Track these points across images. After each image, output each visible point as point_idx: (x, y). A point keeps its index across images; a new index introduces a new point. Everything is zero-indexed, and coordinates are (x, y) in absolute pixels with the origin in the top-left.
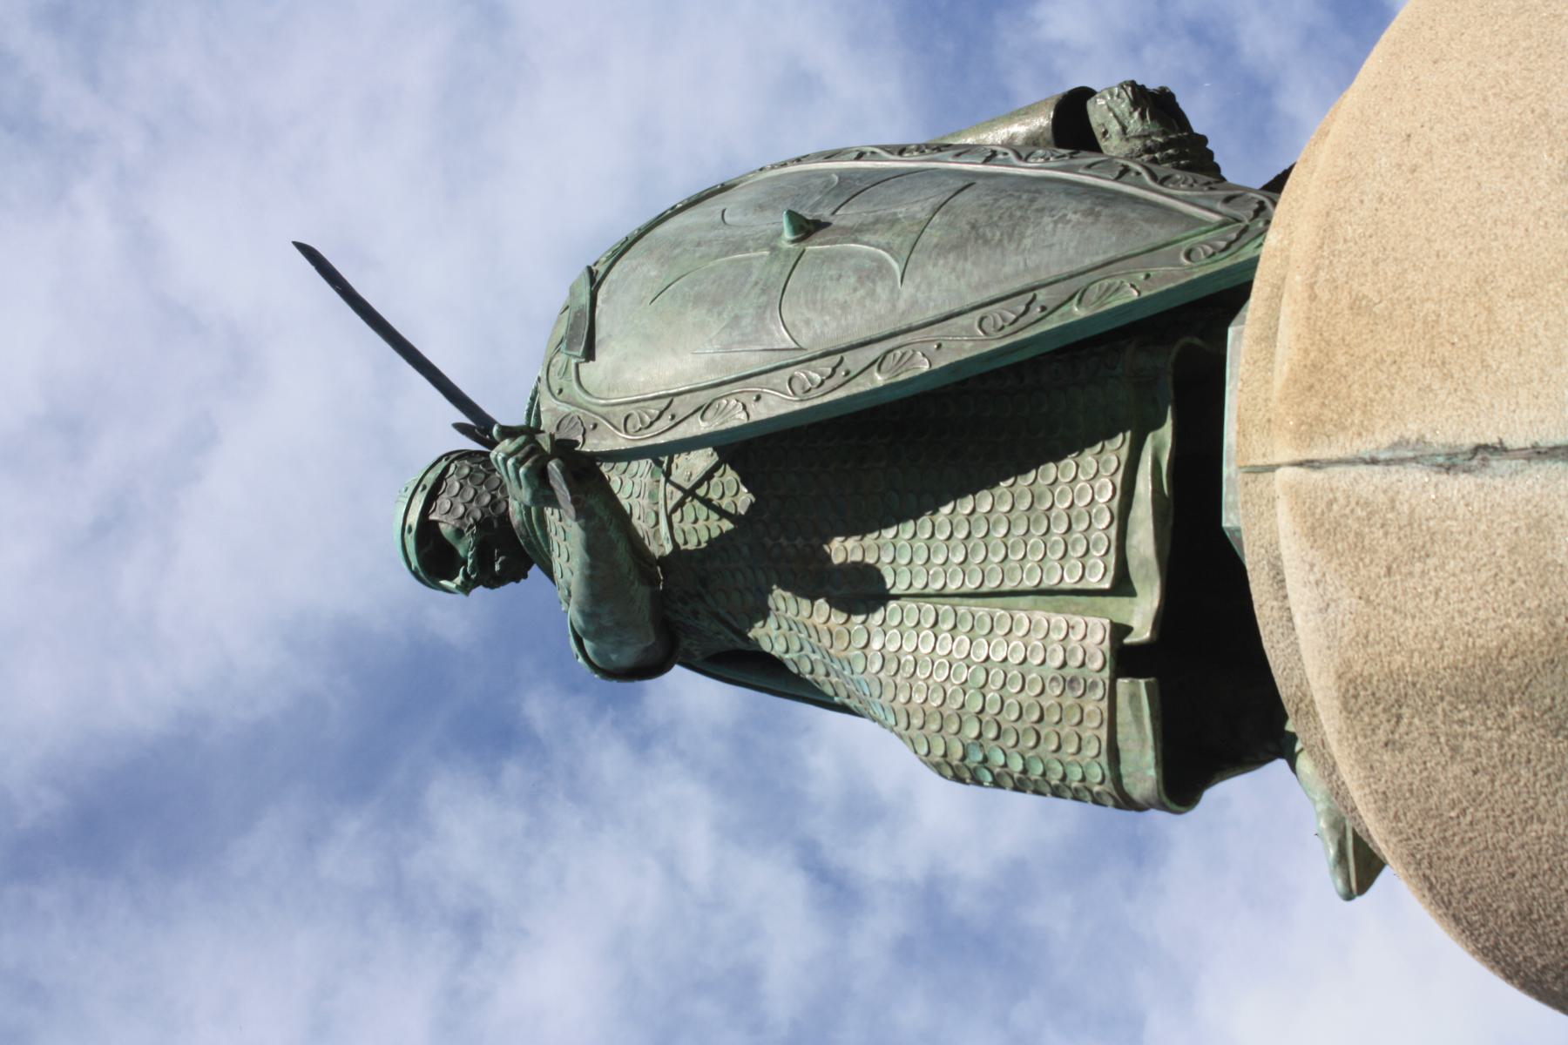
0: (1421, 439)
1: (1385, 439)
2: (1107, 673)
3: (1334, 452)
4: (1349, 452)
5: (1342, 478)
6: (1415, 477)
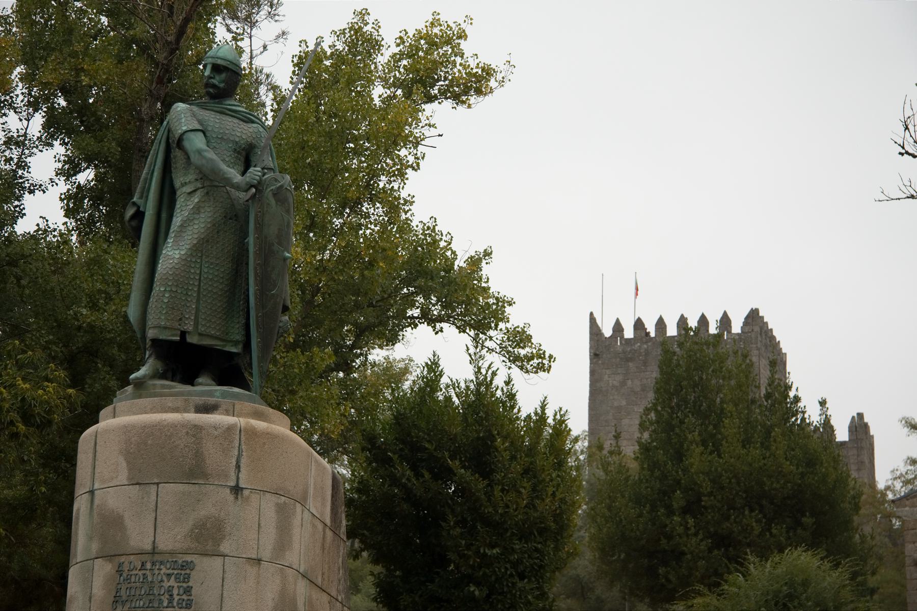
0: (242, 455)
2: (182, 329)
3: (242, 436)
4: (242, 439)
5: (237, 437)
6: (236, 453)
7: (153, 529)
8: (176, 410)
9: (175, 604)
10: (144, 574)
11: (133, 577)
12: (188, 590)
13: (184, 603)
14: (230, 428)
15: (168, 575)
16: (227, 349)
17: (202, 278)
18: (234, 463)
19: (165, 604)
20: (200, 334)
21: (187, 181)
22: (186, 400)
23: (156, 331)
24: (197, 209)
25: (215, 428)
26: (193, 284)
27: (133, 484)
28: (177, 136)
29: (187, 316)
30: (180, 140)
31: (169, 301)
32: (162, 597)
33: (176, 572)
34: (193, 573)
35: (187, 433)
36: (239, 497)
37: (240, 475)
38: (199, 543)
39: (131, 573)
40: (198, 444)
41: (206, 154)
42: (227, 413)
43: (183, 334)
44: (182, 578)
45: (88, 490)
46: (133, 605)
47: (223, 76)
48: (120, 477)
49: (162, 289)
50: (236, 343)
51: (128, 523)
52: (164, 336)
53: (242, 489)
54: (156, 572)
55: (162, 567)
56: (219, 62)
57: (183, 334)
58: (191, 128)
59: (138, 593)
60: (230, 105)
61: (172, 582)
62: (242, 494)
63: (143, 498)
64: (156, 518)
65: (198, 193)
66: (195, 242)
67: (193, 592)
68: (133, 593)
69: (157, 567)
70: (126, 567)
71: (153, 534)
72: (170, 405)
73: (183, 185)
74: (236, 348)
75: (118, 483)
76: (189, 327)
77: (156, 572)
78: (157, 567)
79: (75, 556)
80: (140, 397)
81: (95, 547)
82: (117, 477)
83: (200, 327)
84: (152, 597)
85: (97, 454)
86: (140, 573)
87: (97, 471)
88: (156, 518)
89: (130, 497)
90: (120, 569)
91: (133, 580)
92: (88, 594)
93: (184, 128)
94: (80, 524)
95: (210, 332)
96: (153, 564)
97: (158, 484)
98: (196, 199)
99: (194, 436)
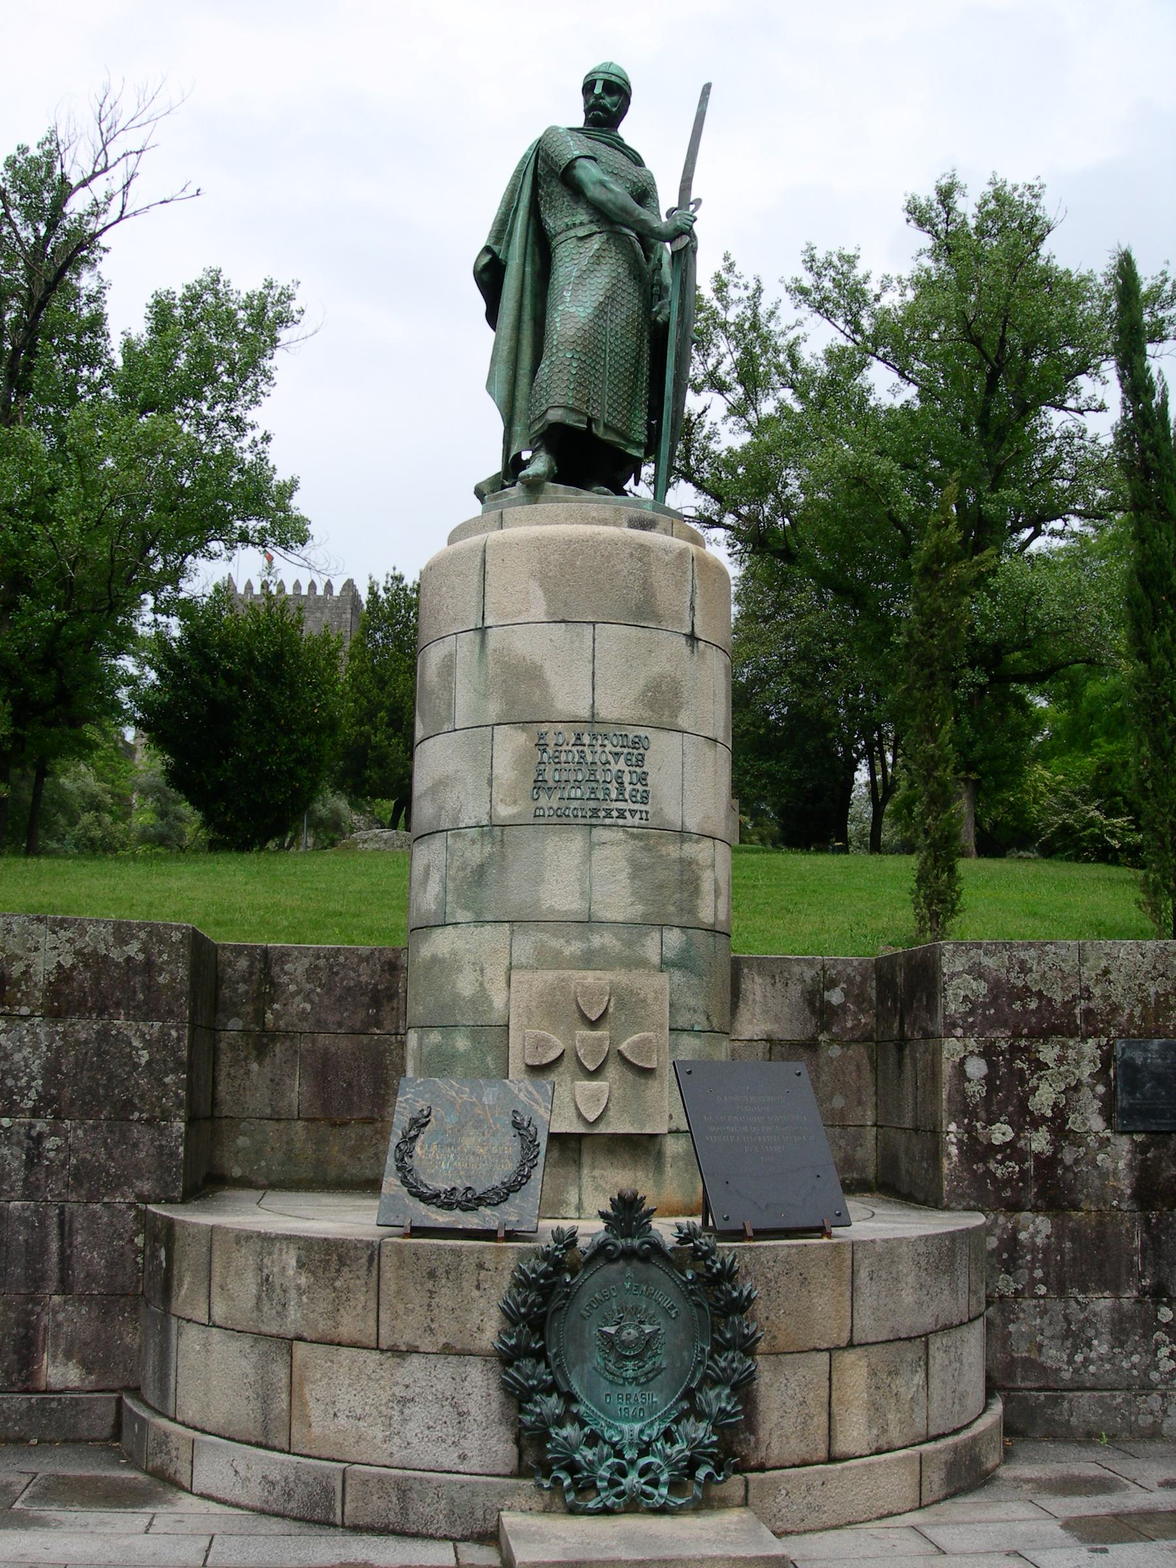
5: (690, 567)
8: (604, 522)
9: (627, 797)
10: (582, 752)
11: (563, 754)
12: (643, 779)
13: (639, 795)
14: (682, 554)
15: (616, 754)
16: (629, 451)
19: (614, 796)
21: (578, 222)
22: (616, 510)
23: (560, 412)
24: (597, 258)
25: (666, 553)
28: (563, 163)
30: (571, 165)
32: (609, 786)
33: (626, 750)
34: (647, 753)
35: (631, 555)
39: (559, 748)
40: (646, 571)
41: (613, 186)
42: (665, 532)
43: (590, 421)
44: (634, 759)
45: (473, 627)
46: (566, 796)
47: (615, 98)
48: (533, 611)
49: (569, 356)
50: (638, 445)
51: (550, 674)
52: (571, 420)
54: (599, 749)
55: (606, 742)
56: (613, 78)
57: (590, 421)
58: (585, 153)
59: (572, 778)
61: (622, 765)
63: (573, 643)
64: (593, 673)
65: (597, 237)
66: (601, 299)
67: (649, 781)
68: (564, 778)
69: (600, 742)
70: (551, 740)
71: (590, 695)
73: (568, 228)
76: (595, 413)
77: (599, 749)
78: (600, 742)
79: (450, 718)
81: (493, 709)
82: (527, 610)
84: (594, 785)
85: (489, 577)
86: (574, 749)
88: (593, 673)
90: (542, 742)
91: (563, 757)
92: (487, 775)
93: (577, 153)
94: (459, 674)
96: (594, 737)
97: (594, 623)
98: (595, 243)
99: (640, 560)
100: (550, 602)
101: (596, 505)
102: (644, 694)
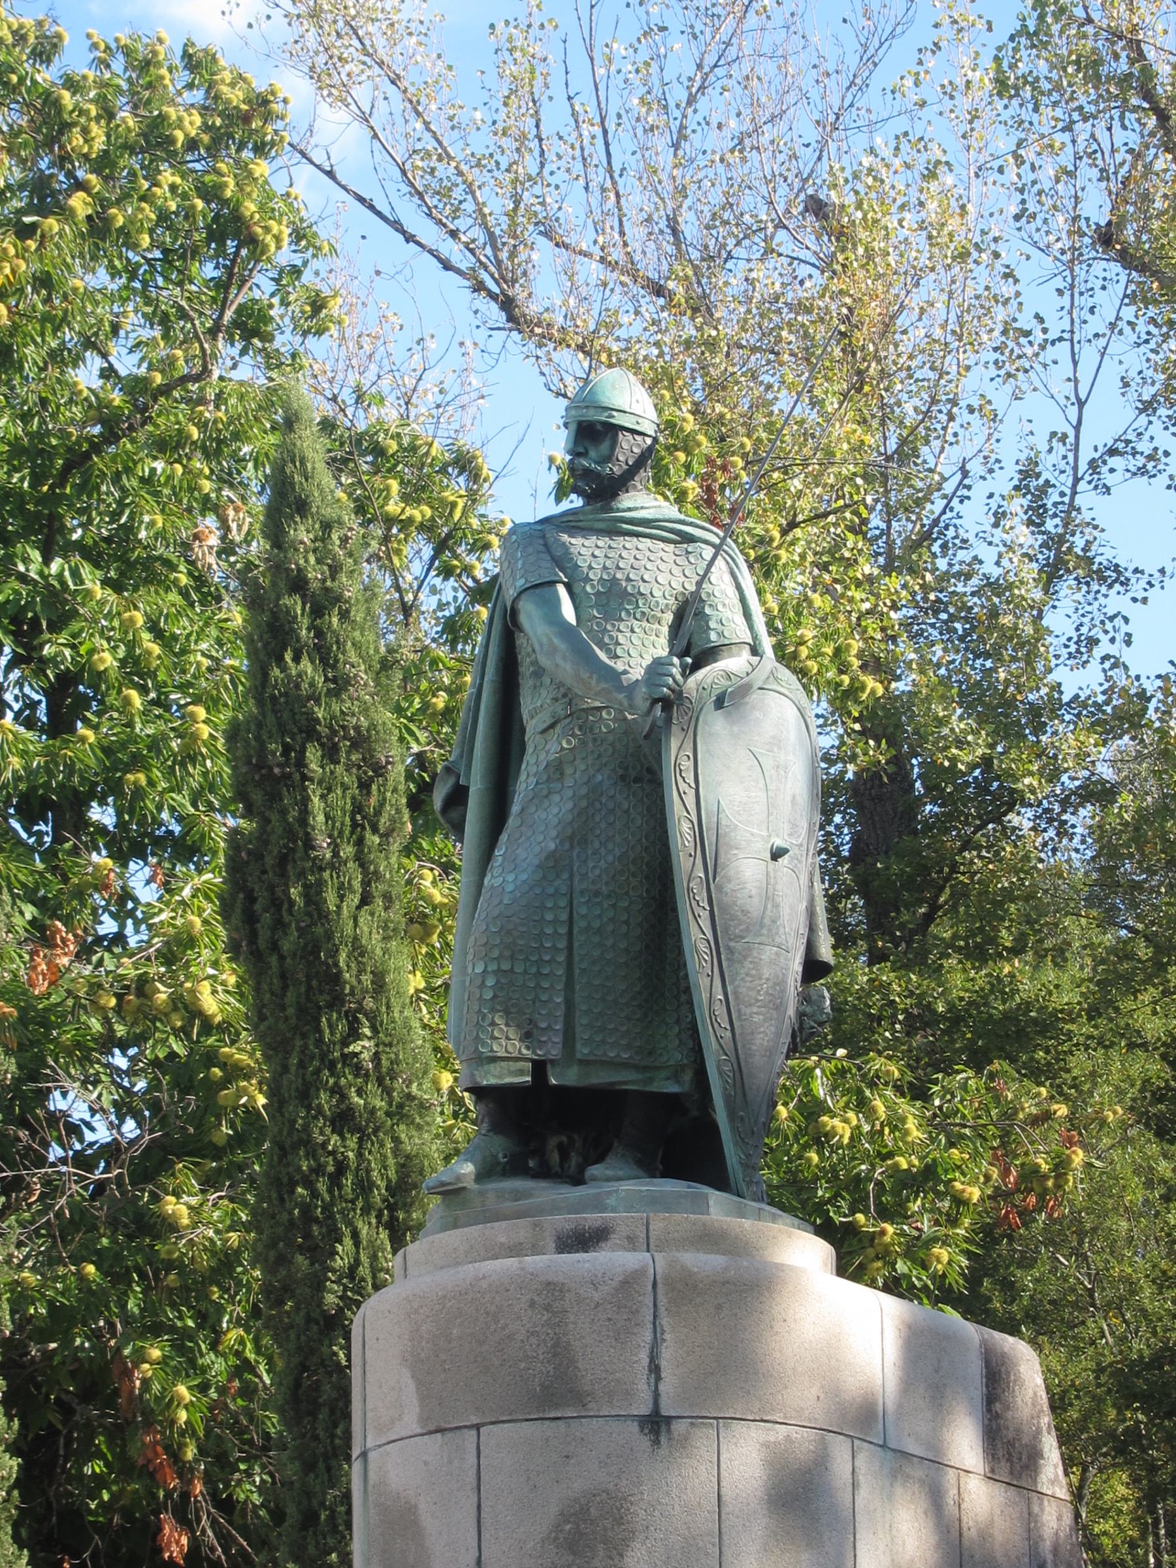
0: (664, 1340)
1: (664, 1322)
4: (660, 1304)
5: (649, 1300)
6: (648, 1336)
7: (474, 1533)
8: (515, 1250)
14: (629, 1282)
17: (575, 931)
18: (646, 1361)
20: (583, 1062)
26: (554, 947)
27: (430, 1433)
29: (543, 1025)
31: (495, 996)
35: (532, 1304)
36: (663, 1439)
37: (662, 1387)
38: (574, 1553)
42: (631, 1243)
43: (539, 1068)
51: (429, 1521)
53: (669, 1420)
60: (630, 510)
62: (669, 1431)
63: (450, 1462)
66: (552, 846)
72: (503, 1240)
74: (678, 1082)
75: (404, 1434)
80: (455, 1226)
83: (578, 1046)
87: (369, 1405)
89: (426, 1463)
95: (605, 1054)
97: (477, 1427)
99: (547, 1308)
100: (423, 1399)
101: (504, 1224)
102: (558, 1528)
